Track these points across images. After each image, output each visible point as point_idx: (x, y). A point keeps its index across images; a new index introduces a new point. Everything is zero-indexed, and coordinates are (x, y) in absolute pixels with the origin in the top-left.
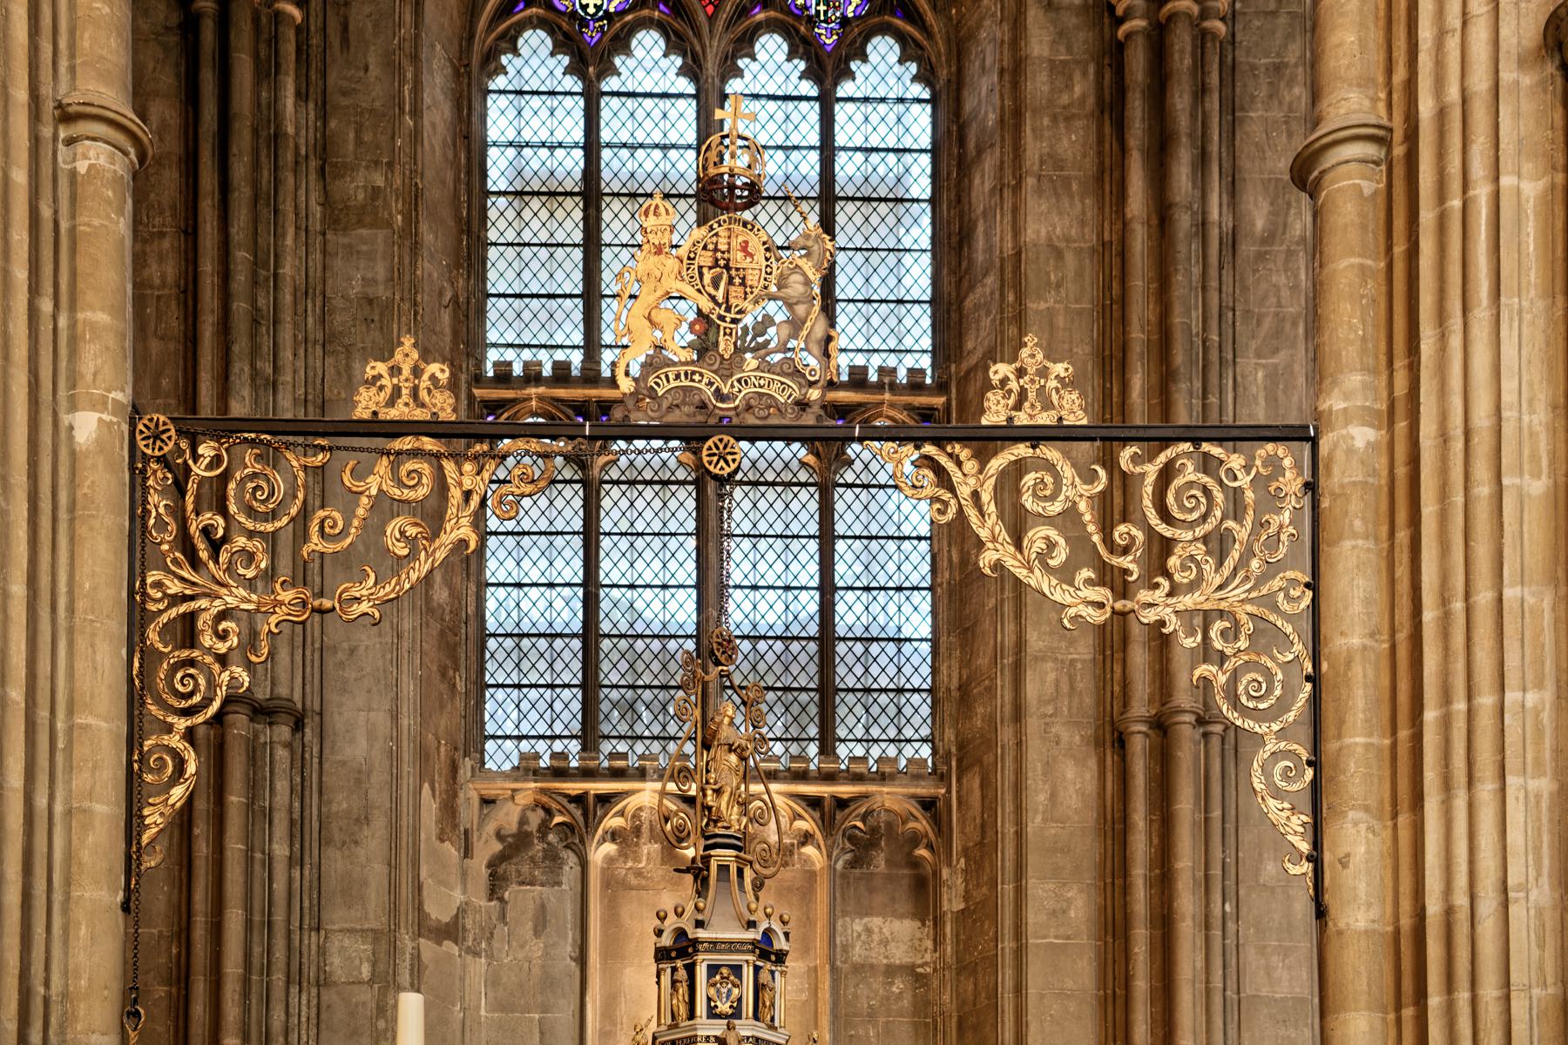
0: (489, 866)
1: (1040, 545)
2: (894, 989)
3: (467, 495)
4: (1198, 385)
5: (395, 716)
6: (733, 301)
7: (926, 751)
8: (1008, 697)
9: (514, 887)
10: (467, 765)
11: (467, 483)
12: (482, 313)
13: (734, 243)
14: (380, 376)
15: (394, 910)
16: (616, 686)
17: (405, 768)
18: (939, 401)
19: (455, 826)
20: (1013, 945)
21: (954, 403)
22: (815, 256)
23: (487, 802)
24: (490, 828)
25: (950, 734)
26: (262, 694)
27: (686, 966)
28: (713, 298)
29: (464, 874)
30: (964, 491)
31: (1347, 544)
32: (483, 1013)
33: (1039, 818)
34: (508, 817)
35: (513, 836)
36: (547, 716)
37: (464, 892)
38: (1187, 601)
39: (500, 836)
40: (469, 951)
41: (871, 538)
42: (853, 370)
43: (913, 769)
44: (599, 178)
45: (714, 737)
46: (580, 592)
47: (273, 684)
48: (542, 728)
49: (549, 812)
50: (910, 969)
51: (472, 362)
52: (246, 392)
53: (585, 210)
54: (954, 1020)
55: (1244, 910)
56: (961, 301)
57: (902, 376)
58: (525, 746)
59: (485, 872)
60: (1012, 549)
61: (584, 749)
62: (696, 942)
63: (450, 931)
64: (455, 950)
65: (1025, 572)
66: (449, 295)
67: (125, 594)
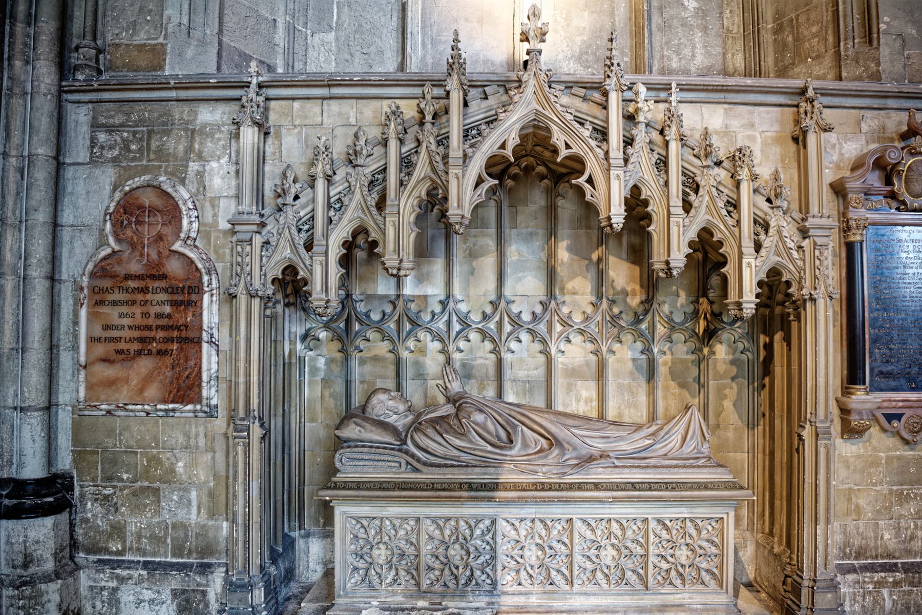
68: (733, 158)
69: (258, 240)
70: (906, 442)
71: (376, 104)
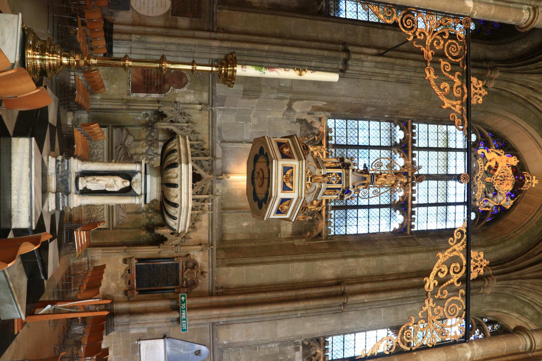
0: (305, 119)
1: (443, 270)
2: (274, 228)
3: (454, 106)
4: (415, 295)
5: (343, 96)
6: (497, 181)
7: (332, 233)
8: (348, 254)
9: (299, 126)
10: (329, 114)
11: (457, 106)
12: (425, 123)
13: (509, 181)
14: (479, 85)
15: (298, 93)
16: (347, 153)
17: (331, 98)
18: (408, 233)
19: (315, 111)
20: (289, 259)
21: (408, 236)
22: (506, 203)
23: (320, 119)
24: (314, 120)
25: (337, 240)
26: (350, 62)
27: (340, 166)
28: (498, 176)
29: (303, 112)
30: (456, 247)
31: (444, 355)
32: (268, 116)
33: (320, 264)
34: (317, 125)
35: (312, 126)
36: (340, 135)
37: (299, 112)
38: (430, 313)
39: (312, 122)
40: (284, 113)
41: (380, 217)
42: (414, 212)
43: (328, 230)
44: (450, 151)
45: (399, 176)
46: (368, 145)
47: (352, 65)
48: (337, 134)
49: (318, 135)
50: (279, 231)
51: (416, 120)
52: (414, 65)
53: (444, 148)
54: (268, 244)
55: (298, 319)
56: (428, 236)
57: (413, 223)
58: (333, 130)
59: (303, 118)
60: (442, 262)
61: (333, 145)
62: (348, 169)
63: (290, 108)
64: (285, 109)
65: (437, 266)
66: (429, 115)
67: (430, 9)
68: (194, 227)
69: (173, 109)
70: (122, 276)
71: (208, 137)
